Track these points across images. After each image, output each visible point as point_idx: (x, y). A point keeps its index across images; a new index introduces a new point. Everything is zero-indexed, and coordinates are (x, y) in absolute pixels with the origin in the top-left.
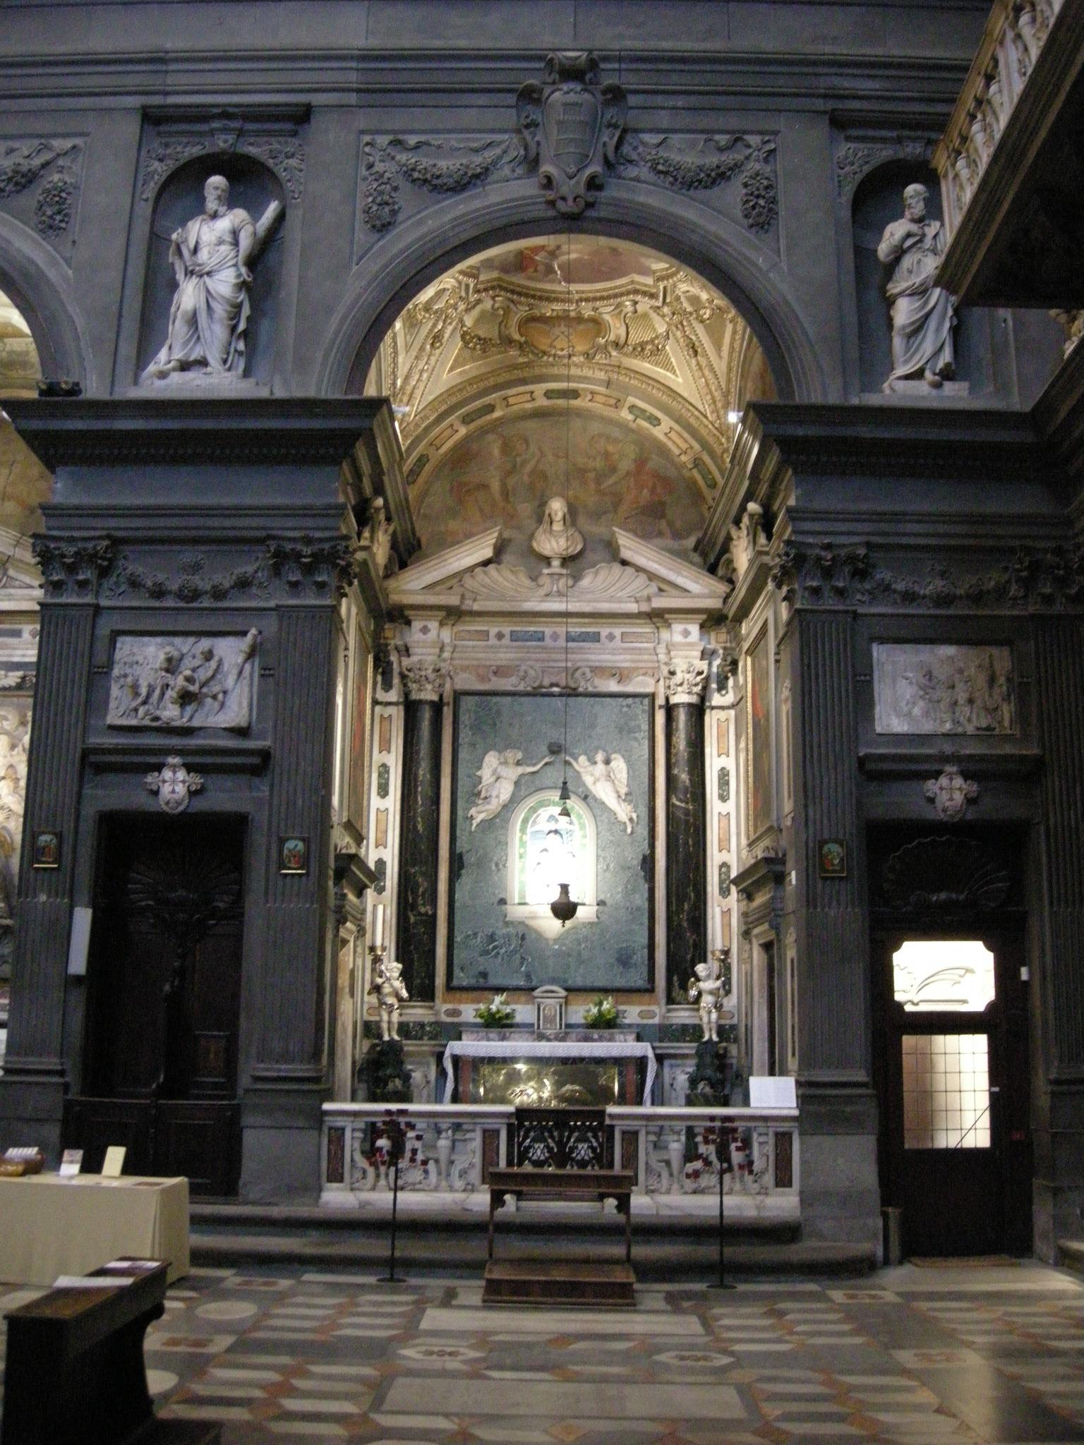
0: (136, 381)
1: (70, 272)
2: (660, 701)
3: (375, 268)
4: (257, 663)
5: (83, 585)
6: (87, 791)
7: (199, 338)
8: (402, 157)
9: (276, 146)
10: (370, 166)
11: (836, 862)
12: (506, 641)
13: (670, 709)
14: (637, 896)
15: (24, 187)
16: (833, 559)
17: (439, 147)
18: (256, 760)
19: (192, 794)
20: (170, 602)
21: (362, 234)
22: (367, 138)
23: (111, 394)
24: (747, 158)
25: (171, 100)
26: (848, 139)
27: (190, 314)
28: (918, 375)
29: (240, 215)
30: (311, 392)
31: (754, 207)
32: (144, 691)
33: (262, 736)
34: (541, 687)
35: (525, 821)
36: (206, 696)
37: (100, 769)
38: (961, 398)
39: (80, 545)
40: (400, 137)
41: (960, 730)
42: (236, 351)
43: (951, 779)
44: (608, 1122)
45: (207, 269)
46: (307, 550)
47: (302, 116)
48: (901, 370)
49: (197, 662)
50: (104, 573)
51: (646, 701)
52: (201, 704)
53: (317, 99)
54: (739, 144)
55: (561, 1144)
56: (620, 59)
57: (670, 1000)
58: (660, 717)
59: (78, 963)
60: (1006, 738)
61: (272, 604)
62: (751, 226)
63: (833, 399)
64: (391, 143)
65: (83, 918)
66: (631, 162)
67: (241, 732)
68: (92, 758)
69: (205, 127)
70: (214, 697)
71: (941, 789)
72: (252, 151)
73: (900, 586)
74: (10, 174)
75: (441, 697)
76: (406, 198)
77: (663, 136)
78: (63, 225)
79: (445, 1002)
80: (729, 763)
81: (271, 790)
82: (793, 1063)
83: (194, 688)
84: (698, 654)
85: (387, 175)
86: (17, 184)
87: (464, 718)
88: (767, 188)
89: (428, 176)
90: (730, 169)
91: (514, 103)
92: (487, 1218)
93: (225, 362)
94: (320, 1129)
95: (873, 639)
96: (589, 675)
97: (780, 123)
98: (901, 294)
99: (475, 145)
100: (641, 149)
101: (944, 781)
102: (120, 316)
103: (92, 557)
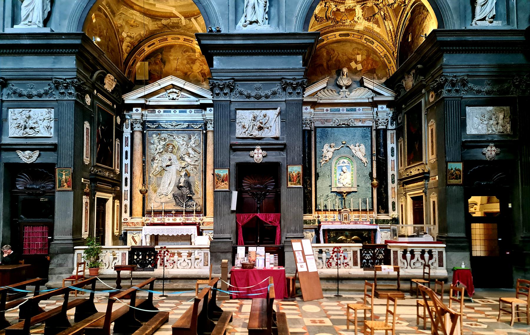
4: (280, 118)
5: (226, 94)
12: (329, 112)
18: (282, 147)
20: (252, 99)
33: (283, 139)
35: (336, 163)
37: (235, 150)
41: (494, 133)
43: (491, 148)
46: (295, 83)
50: (232, 90)
51: (370, 128)
57: (378, 212)
58: (374, 133)
59: (234, 207)
60: (508, 135)
61: (284, 100)
67: (277, 138)
68: (233, 147)
70: (268, 128)
71: (488, 151)
81: (287, 155)
83: (262, 126)
87: (318, 135)
96: (353, 121)
101: (489, 148)
103: (228, 86)
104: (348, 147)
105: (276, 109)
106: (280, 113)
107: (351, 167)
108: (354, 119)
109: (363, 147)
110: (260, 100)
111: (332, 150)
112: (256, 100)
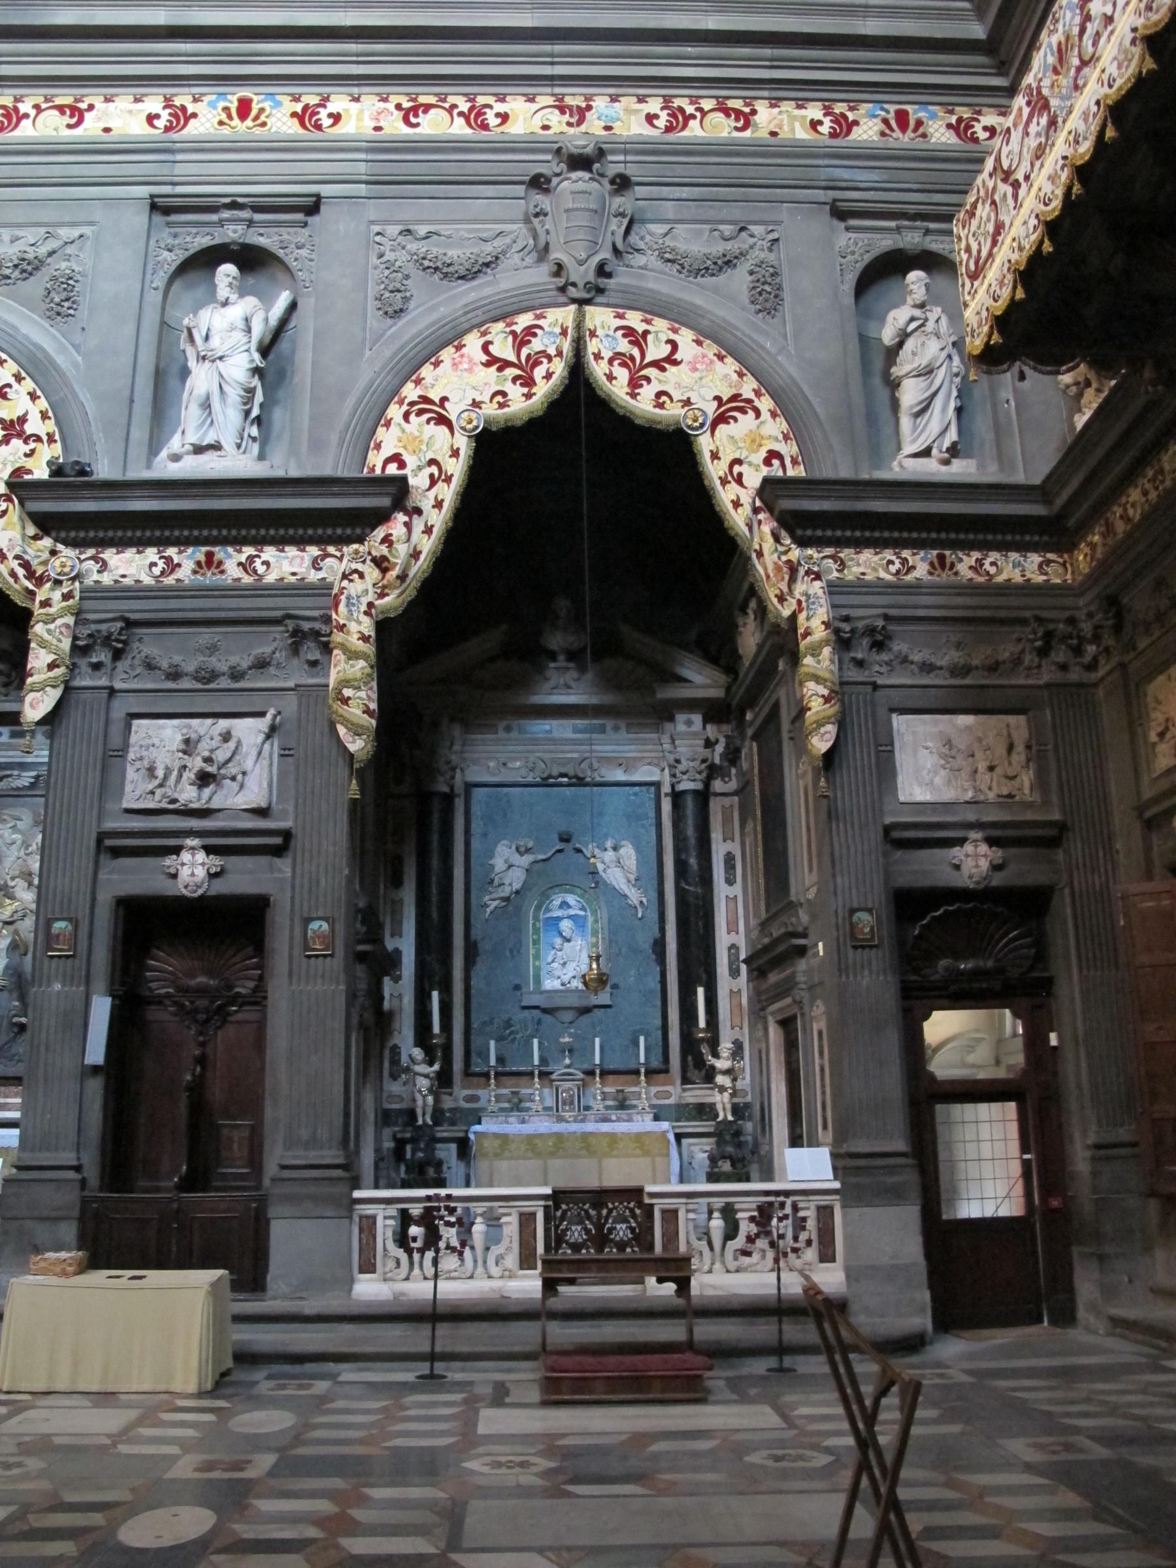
0: (149, 466)
1: (80, 359)
2: (666, 788)
3: (388, 353)
4: (276, 744)
5: (97, 667)
6: (102, 876)
7: (212, 421)
8: (413, 246)
9: (286, 237)
10: (381, 256)
11: (867, 930)
13: (677, 797)
14: (650, 979)
15: (31, 274)
16: (853, 631)
17: (449, 237)
18: (278, 840)
19: (212, 876)
20: (185, 684)
21: (374, 320)
22: (376, 228)
23: (124, 475)
24: (751, 247)
25: (180, 190)
26: (847, 229)
27: (204, 398)
28: (926, 453)
29: (251, 301)
30: (327, 471)
31: (760, 294)
32: (160, 773)
33: (284, 815)
34: (550, 777)
35: (538, 908)
36: (224, 777)
38: (970, 474)
39: (93, 627)
40: (411, 227)
41: (982, 798)
42: (249, 436)
43: (976, 847)
44: (647, 1201)
45: (220, 354)
47: (313, 207)
48: (909, 448)
49: (214, 744)
50: (117, 655)
51: (652, 789)
52: (219, 785)
53: (325, 190)
54: (744, 234)
55: (600, 1227)
56: (626, 152)
57: (685, 1080)
58: (666, 805)
59: (96, 1053)
61: (291, 684)
62: (760, 311)
63: (845, 473)
64: (400, 233)
65: (101, 1009)
66: (638, 251)
67: (261, 812)
68: (109, 842)
69: (214, 217)
70: (233, 779)
71: (967, 856)
72: (262, 241)
73: (916, 657)
74: (16, 262)
75: (452, 788)
76: (417, 284)
77: (669, 226)
78: (71, 312)
79: (464, 1088)
80: (735, 848)
82: (828, 1136)
83: (210, 769)
84: (702, 742)
85: (398, 264)
86: (24, 271)
87: (476, 809)
88: (772, 275)
89: (439, 264)
90: (736, 257)
91: (522, 194)
92: (539, 1306)
93: (239, 446)
94: (350, 1217)
95: (892, 710)
96: (596, 765)
97: (784, 212)
98: (906, 375)
99: (484, 235)
100: (648, 238)
101: (969, 848)
102: (132, 401)
103: (107, 640)
104: (579, 851)
105: (262, 714)
106: (273, 730)
107: (590, 919)
108: (601, 759)
109: (628, 852)
110: (212, 686)
111: (527, 859)
112: (199, 686)
